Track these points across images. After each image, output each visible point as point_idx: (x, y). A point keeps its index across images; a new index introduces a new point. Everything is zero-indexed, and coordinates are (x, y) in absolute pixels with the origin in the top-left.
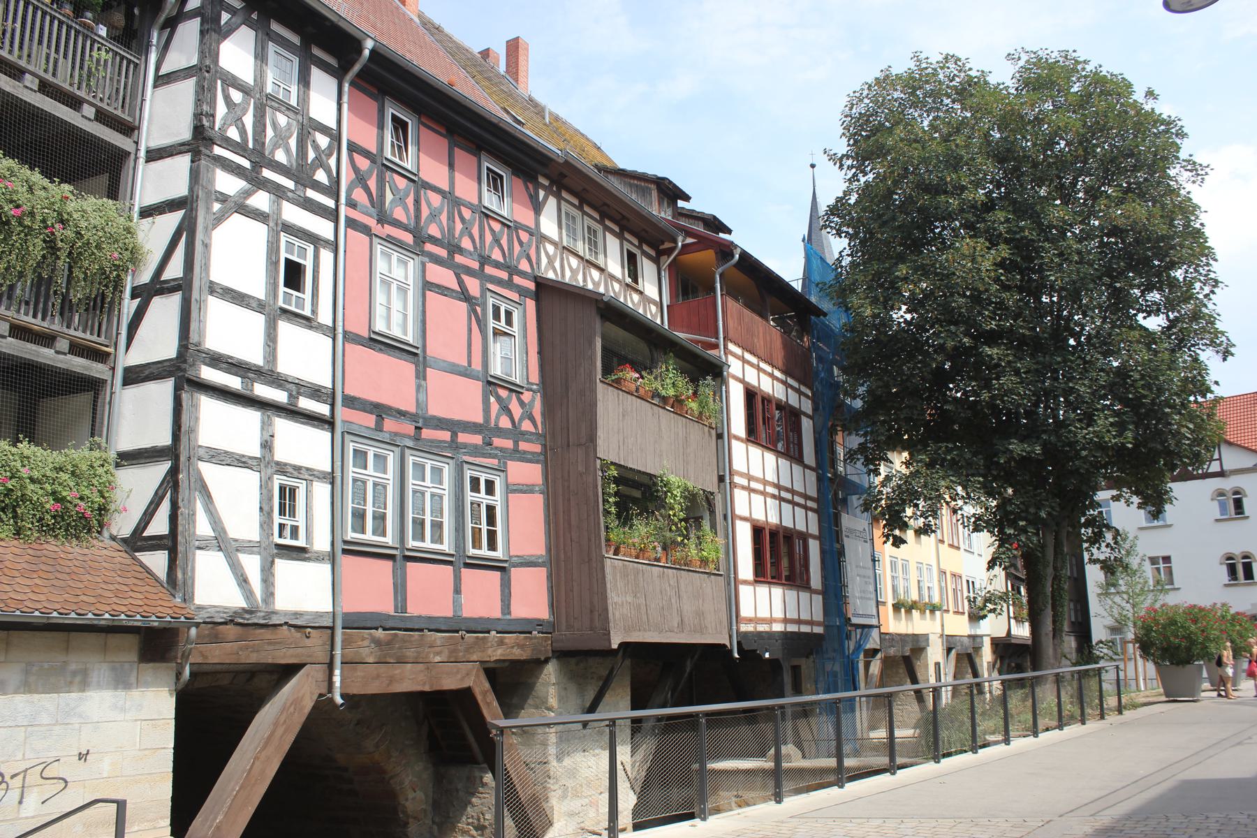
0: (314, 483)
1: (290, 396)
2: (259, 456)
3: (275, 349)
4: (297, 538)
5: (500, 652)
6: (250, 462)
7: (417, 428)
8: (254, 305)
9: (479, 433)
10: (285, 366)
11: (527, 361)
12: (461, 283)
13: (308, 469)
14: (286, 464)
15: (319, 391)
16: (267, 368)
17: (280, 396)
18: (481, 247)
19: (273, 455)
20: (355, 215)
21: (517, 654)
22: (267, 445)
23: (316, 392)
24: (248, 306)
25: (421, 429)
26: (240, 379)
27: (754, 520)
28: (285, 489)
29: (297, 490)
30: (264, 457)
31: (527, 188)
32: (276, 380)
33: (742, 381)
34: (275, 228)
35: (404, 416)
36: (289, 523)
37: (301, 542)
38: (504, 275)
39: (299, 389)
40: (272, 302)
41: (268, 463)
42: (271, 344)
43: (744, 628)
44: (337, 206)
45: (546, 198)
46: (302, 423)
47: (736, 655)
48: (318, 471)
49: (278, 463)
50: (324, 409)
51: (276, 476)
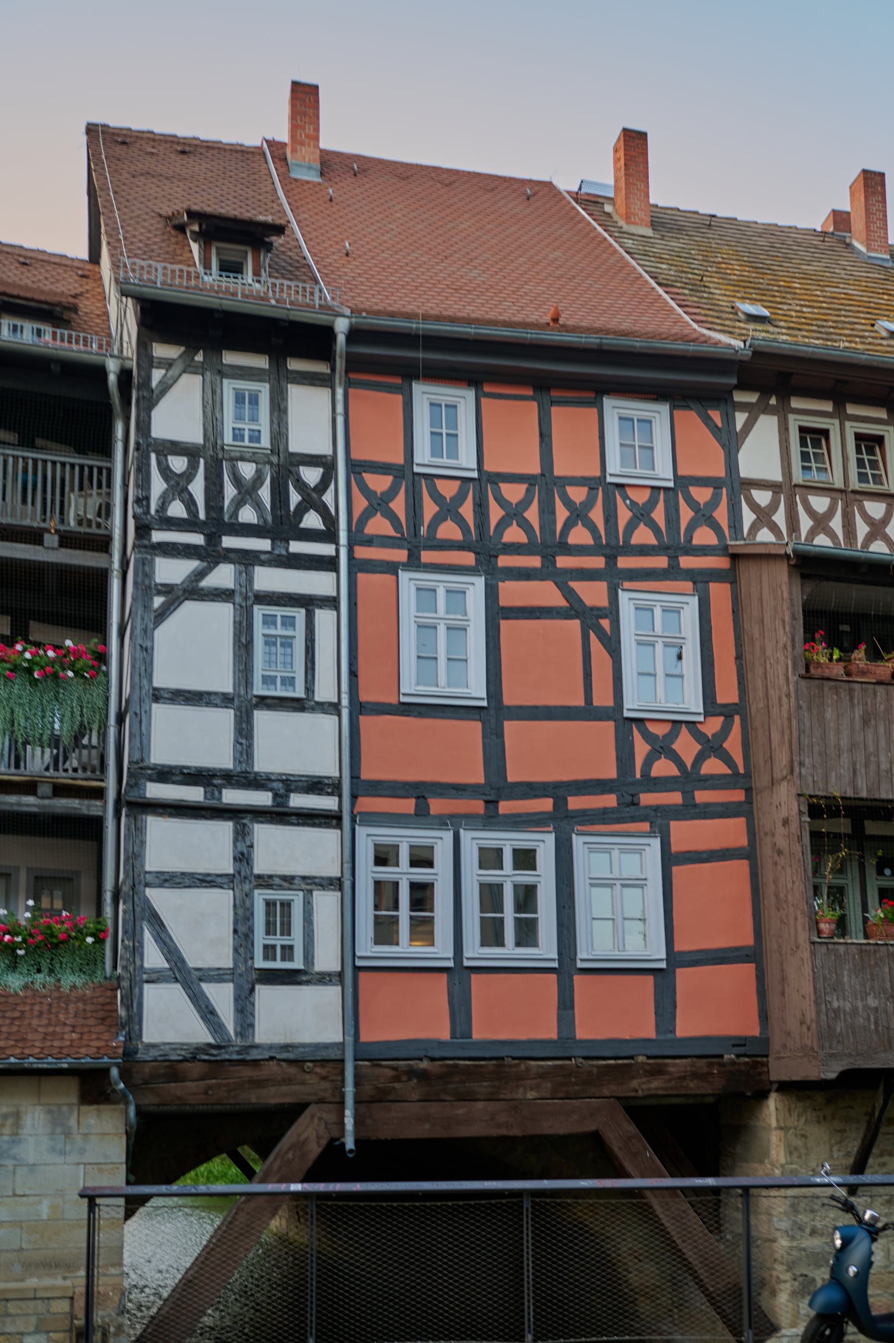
0: (315, 893)
1: (276, 796)
2: (231, 871)
3: (250, 746)
4: (291, 959)
6: (219, 880)
7: (486, 802)
8: (218, 701)
9: (610, 791)
10: (262, 764)
12: (569, 594)
13: (304, 878)
14: (270, 877)
15: (319, 783)
16: (239, 769)
17: (263, 799)
19: (252, 868)
20: (362, 553)
22: (243, 858)
23: (315, 786)
24: (209, 704)
25: (497, 802)
26: (201, 789)
28: (275, 904)
29: (292, 903)
30: (239, 873)
31: (708, 421)
32: (256, 782)
34: (244, 604)
35: (464, 790)
36: (278, 941)
37: (298, 963)
39: (289, 785)
40: (242, 692)
41: (246, 878)
42: (244, 741)
44: (337, 551)
46: (298, 825)
48: (322, 878)
49: (259, 877)
50: (328, 803)
51: (256, 892)
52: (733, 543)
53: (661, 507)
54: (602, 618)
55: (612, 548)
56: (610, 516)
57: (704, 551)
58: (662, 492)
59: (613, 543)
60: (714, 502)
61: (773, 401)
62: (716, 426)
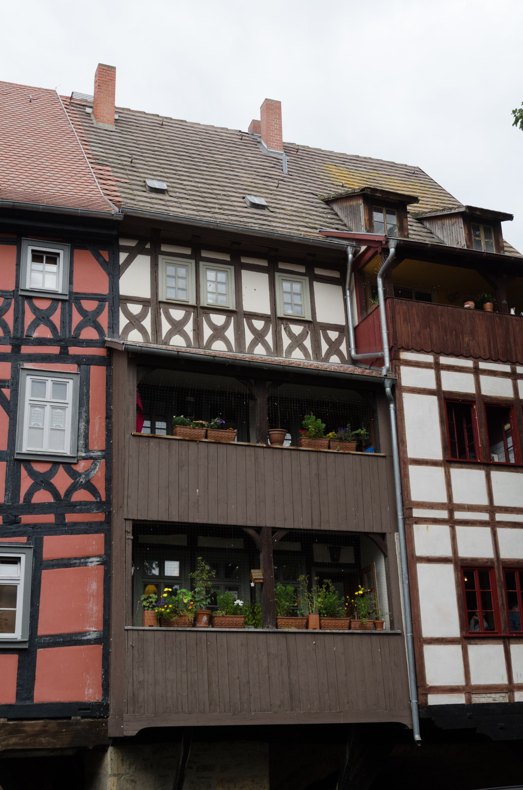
5: (13, 740)
11: (87, 429)
18: (16, 329)
21: (44, 741)
27: (464, 560)
31: (98, 257)
33: (438, 392)
38: (55, 350)
43: (434, 700)
45: (128, 261)
47: (417, 737)
52: (109, 339)
53: (58, 312)
54: (4, 387)
55: (17, 339)
56: (19, 318)
57: (89, 343)
58: (60, 304)
59: (19, 335)
60: (98, 311)
61: (148, 246)
62: (105, 261)
